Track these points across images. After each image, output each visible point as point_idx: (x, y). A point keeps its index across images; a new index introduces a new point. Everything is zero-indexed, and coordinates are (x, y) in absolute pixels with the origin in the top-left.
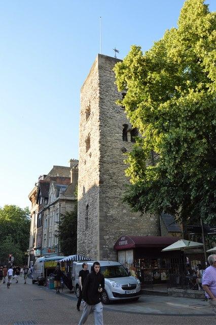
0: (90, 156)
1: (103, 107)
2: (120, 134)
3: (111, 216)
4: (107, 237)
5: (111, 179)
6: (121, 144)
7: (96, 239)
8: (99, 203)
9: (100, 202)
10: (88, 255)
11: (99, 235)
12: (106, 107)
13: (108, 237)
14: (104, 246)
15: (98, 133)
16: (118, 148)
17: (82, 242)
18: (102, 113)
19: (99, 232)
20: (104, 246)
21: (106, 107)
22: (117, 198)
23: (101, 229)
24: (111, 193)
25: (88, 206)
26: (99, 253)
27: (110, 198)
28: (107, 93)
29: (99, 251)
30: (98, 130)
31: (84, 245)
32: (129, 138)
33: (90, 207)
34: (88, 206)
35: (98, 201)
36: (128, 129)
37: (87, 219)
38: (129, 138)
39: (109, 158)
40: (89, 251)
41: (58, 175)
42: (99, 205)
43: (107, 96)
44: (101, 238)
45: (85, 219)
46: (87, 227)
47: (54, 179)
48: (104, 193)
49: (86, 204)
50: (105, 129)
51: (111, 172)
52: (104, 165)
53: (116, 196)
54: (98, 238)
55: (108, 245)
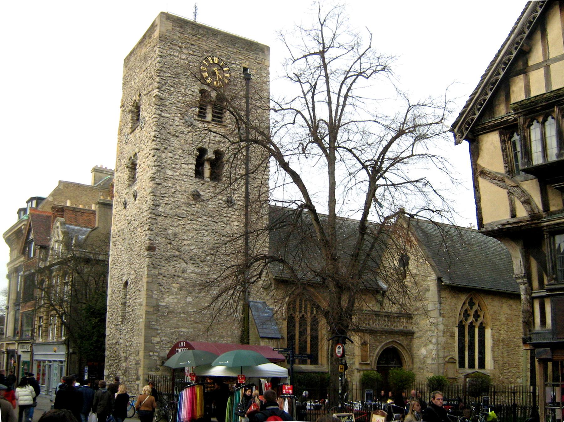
0: (135, 196)
1: (163, 114)
2: (190, 166)
3: (166, 307)
4: (158, 339)
5: (170, 243)
7: (139, 341)
8: (145, 284)
9: (147, 282)
10: (124, 364)
11: (143, 334)
12: (168, 115)
13: (158, 339)
14: (151, 354)
15: (150, 161)
16: (185, 192)
17: (114, 341)
18: (161, 126)
19: (143, 331)
20: (151, 354)
21: (168, 115)
22: (179, 276)
23: (148, 326)
24: (168, 269)
25: (126, 284)
26: (142, 363)
27: (165, 276)
28: (172, 89)
29: (142, 360)
30: (151, 156)
31: (118, 346)
32: (207, 173)
33: (131, 287)
34: (126, 284)
35: (145, 280)
36: (206, 157)
37: (124, 304)
38: (207, 173)
39: (169, 207)
40: (126, 358)
41: (68, 204)
42: (145, 287)
43: (171, 95)
44: (147, 340)
45: (122, 304)
46: (124, 319)
47: (60, 211)
48: (154, 268)
49: (125, 279)
50: (164, 155)
51: (170, 232)
52: (159, 219)
53: (176, 274)
54: (142, 339)
55: (157, 352)
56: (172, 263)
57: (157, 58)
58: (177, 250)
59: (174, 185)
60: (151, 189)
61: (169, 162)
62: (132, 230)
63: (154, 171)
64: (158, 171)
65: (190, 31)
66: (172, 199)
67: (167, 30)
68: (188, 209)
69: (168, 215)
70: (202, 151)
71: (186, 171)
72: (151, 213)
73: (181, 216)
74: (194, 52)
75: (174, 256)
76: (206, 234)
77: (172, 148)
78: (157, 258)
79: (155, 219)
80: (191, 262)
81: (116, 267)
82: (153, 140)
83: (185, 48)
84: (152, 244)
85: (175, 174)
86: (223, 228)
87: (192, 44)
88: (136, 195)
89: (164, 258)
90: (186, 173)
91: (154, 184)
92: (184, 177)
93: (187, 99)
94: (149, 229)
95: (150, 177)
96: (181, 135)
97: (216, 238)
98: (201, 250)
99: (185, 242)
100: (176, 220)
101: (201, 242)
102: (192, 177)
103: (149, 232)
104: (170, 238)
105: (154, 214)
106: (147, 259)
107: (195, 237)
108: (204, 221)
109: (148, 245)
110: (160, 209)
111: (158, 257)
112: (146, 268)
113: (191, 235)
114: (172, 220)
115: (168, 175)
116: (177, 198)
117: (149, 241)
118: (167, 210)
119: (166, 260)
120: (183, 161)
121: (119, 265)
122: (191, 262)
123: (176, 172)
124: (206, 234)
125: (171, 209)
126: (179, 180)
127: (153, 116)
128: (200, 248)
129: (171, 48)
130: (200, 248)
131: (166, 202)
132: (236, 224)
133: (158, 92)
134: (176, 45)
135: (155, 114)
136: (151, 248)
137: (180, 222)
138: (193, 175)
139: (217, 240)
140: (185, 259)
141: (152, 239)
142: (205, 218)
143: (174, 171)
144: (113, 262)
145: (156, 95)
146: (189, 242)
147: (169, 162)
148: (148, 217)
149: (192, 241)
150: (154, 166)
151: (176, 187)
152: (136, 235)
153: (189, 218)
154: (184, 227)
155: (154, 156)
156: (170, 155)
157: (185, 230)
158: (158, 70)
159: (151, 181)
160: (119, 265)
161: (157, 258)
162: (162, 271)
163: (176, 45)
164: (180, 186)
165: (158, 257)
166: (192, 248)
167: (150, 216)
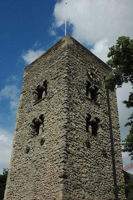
2: (84, 124)
5: (75, 174)
6: (84, 136)
38: (90, 130)
56: (77, 190)
57: (66, 57)
58: (79, 180)
59: (76, 134)
60: (64, 133)
61: (73, 118)
62: (39, 165)
63: (66, 122)
64: (68, 122)
65: (81, 48)
66: (75, 143)
67: (71, 44)
68: (84, 152)
69: (74, 153)
70: (89, 116)
71: (82, 126)
72: (65, 150)
73: (80, 155)
74: (83, 60)
75: (78, 185)
76: (94, 171)
77: (75, 110)
78: (68, 185)
79: (67, 155)
80: (87, 190)
81: (15, 196)
82: (65, 103)
83: (79, 56)
84: (65, 173)
85: (77, 127)
86: (102, 168)
87: (82, 56)
88: (44, 141)
89: (72, 185)
90: (82, 128)
91: (66, 130)
92: (81, 130)
93: (81, 84)
94: (63, 162)
95: (63, 125)
96: (78, 104)
97: (99, 175)
98: (92, 182)
99: (83, 175)
100: (78, 158)
101: (92, 176)
102: (85, 131)
103: (63, 164)
104: (75, 170)
105: (66, 151)
106: (62, 184)
107: (88, 172)
108: (92, 162)
109: (63, 173)
110: (69, 148)
111: (69, 184)
112: (61, 192)
113: (86, 170)
114: (76, 157)
115: (73, 126)
116: (78, 142)
117: (63, 170)
118: (73, 150)
119: (73, 187)
120: (80, 120)
121: (19, 194)
122: (87, 190)
123: (77, 126)
124: (94, 171)
125: (75, 150)
126: (79, 131)
127: (65, 88)
128: (91, 181)
129: (73, 54)
130: (91, 181)
131: (72, 144)
132: (108, 167)
133: (67, 75)
134: (75, 53)
135: (66, 87)
136: (65, 176)
137: (80, 160)
138: (85, 130)
139: (99, 176)
140: (84, 187)
141: (65, 169)
142: (93, 159)
143: (76, 124)
144: (11, 193)
145: (66, 77)
146: (85, 175)
147: (73, 118)
148: (62, 152)
149: (87, 175)
150: (66, 118)
151: (77, 136)
152: (44, 168)
153: (85, 158)
154: (82, 163)
155: (65, 112)
156: (74, 114)
157: (82, 166)
158: (67, 63)
159: (64, 128)
160: (19, 194)
161: (68, 185)
162: (71, 196)
163: (75, 53)
164: (80, 136)
165: (69, 184)
166: (87, 179)
167: (64, 152)
